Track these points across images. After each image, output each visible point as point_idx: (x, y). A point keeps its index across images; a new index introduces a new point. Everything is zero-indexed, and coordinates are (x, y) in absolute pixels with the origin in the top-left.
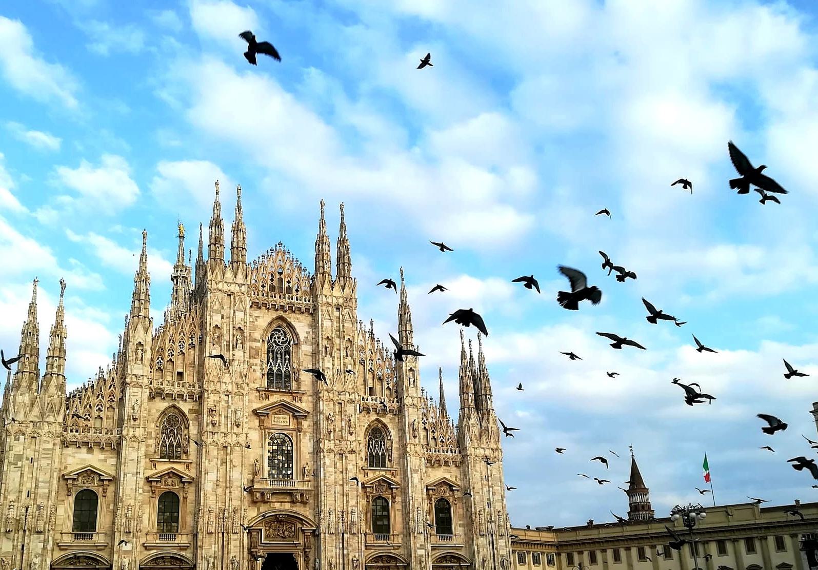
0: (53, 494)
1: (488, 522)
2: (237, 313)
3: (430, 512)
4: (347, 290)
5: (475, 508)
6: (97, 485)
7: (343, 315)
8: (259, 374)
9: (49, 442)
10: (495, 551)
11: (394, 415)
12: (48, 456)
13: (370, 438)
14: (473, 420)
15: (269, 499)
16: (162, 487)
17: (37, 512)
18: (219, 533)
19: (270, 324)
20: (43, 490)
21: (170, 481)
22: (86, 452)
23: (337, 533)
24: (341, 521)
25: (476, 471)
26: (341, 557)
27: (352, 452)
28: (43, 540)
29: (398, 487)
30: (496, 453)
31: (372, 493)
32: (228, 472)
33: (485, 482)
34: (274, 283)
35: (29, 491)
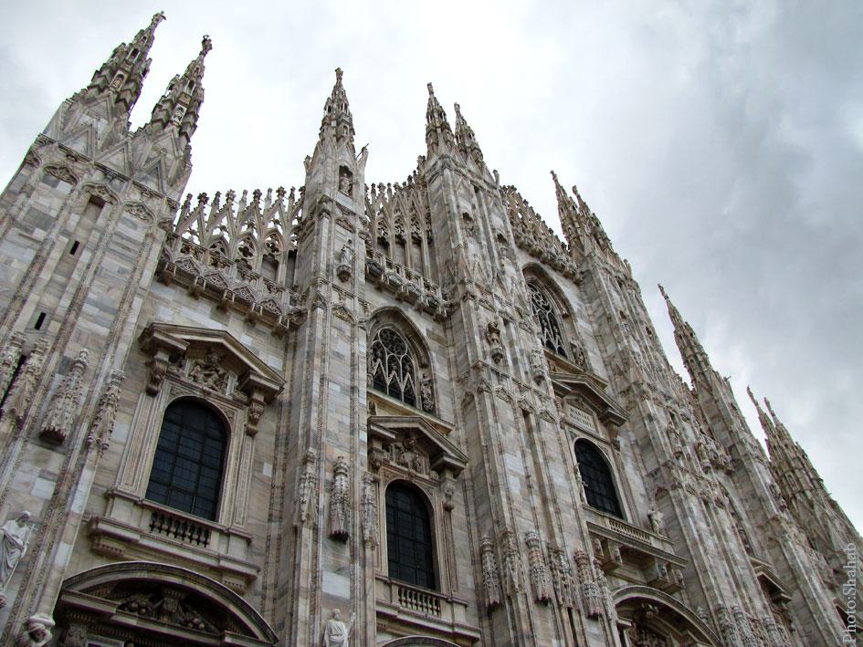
0: (124, 347)
2: (493, 216)
6: (230, 398)
9: (135, 226)
11: (729, 473)
12: (128, 253)
16: (392, 463)
17: (58, 377)
18: (560, 607)
21: (408, 457)
22: (209, 312)
28: (57, 471)
32: (543, 467)
35: (43, 316)
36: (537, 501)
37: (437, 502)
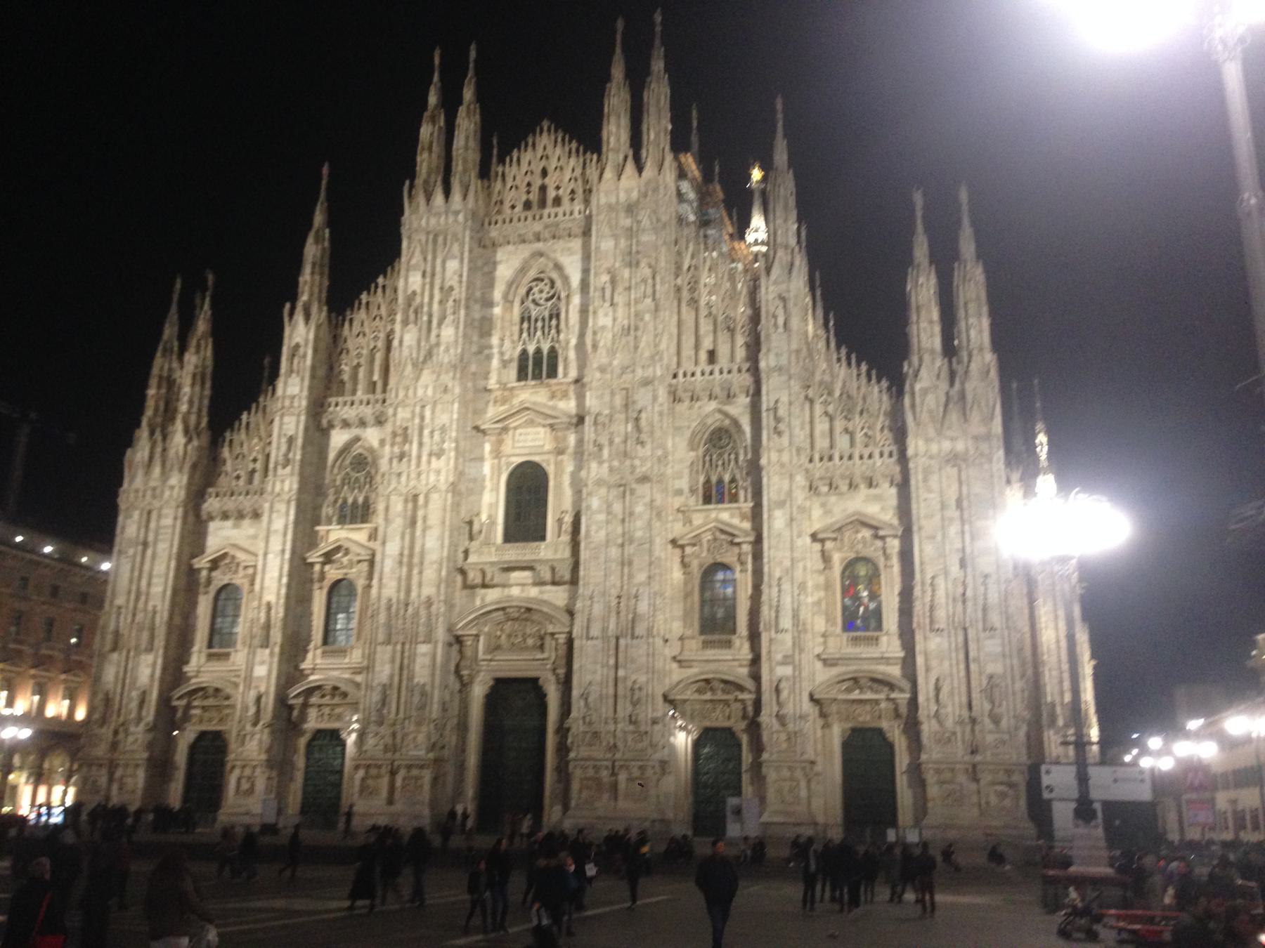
0: (169, 593)
1: (954, 600)
3: (828, 586)
4: (649, 172)
5: (922, 571)
7: (639, 222)
9: (166, 516)
10: (973, 667)
13: (708, 450)
15: (492, 579)
19: (523, 270)
20: (157, 589)
23: (605, 638)
24: (613, 615)
25: (930, 491)
26: (611, 684)
27: (644, 479)
29: (751, 539)
30: (984, 447)
31: (698, 556)
33: (952, 512)
34: (531, 196)
37: (360, 583)
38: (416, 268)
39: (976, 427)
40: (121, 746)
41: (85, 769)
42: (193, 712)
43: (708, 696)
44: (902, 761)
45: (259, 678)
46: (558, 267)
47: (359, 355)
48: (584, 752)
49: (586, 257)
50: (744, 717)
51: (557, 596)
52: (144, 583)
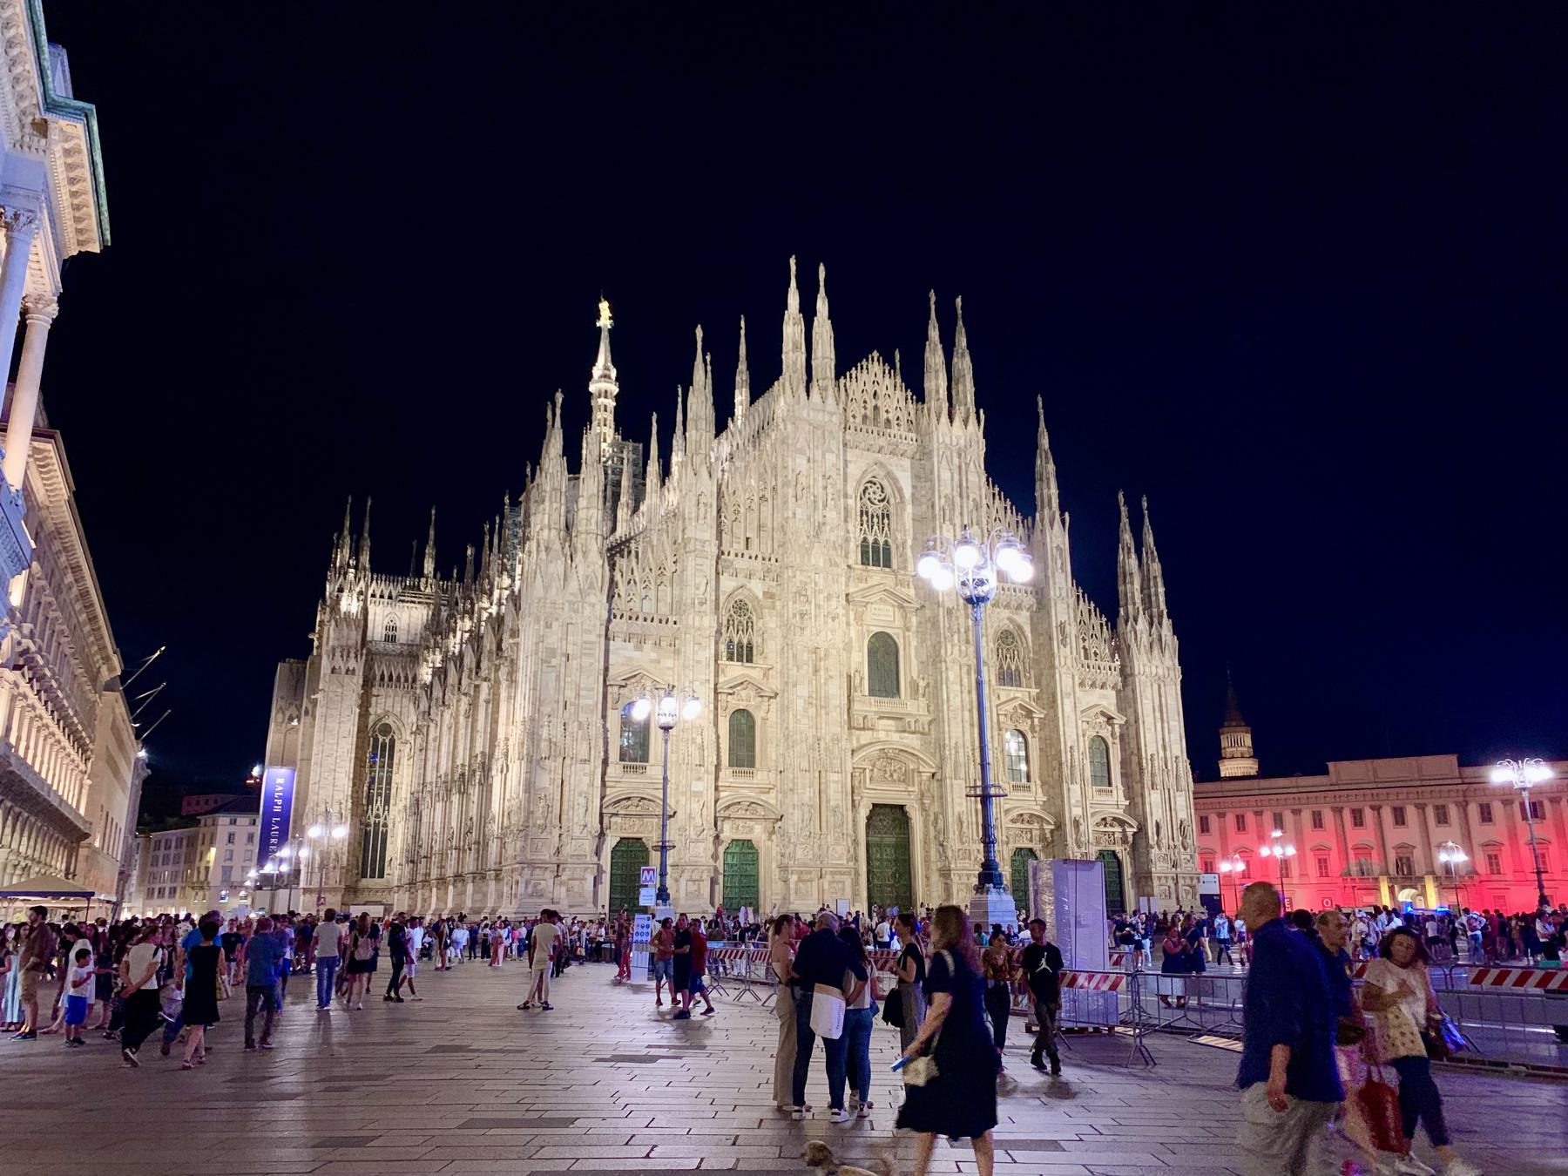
7: (967, 465)
8: (852, 545)
14: (1142, 624)
36: (812, 711)
37: (758, 717)
38: (801, 451)
39: (1168, 662)
40: (567, 850)
41: (527, 872)
42: (614, 819)
43: (1019, 825)
44: (1128, 871)
45: (698, 794)
46: (889, 475)
47: (737, 512)
48: (960, 864)
49: (923, 476)
50: (1043, 838)
51: (913, 742)
52: (570, 694)
